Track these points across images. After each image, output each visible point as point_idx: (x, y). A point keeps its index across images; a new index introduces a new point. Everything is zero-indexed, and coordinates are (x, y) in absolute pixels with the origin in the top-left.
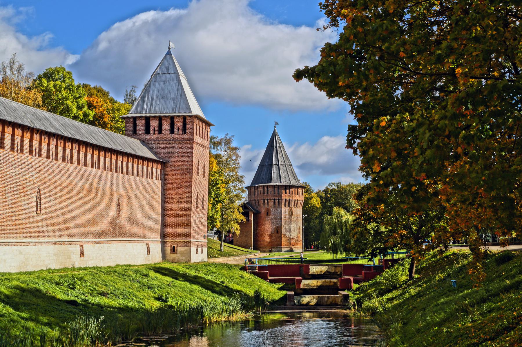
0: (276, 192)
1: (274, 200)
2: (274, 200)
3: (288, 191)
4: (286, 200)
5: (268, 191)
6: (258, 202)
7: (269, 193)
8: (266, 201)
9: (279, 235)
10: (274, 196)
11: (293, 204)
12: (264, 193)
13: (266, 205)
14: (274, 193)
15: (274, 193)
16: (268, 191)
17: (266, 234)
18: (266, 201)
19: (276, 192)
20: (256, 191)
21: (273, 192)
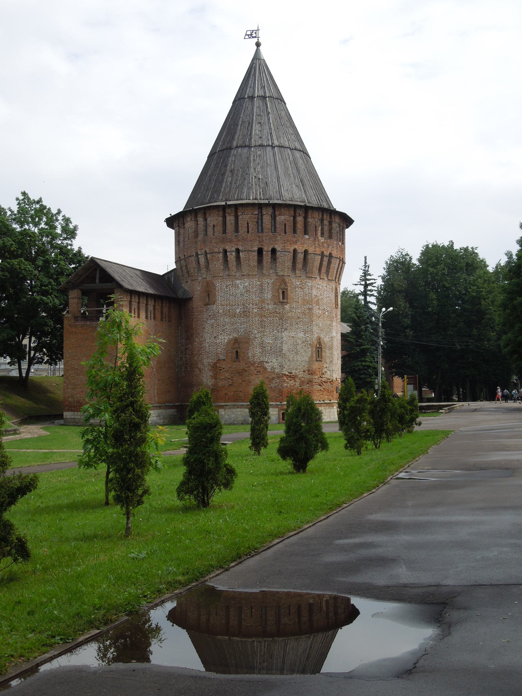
0: (230, 227)
1: (225, 252)
2: (225, 252)
3: (267, 219)
4: (260, 251)
5: (206, 226)
6: (186, 266)
7: (210, 230)
8: (202, 260)
9: (242, 365)
10: (224, 241)
11: (289, 264)
12: (196, 235)
13: (203, 271)
14: (224, 232)
15: (224, 232)
16: (206, 226)
17: (205, 361)
18: (202, 260)
19: (230, 227)
20: (182, 231)
21: (219, 228)
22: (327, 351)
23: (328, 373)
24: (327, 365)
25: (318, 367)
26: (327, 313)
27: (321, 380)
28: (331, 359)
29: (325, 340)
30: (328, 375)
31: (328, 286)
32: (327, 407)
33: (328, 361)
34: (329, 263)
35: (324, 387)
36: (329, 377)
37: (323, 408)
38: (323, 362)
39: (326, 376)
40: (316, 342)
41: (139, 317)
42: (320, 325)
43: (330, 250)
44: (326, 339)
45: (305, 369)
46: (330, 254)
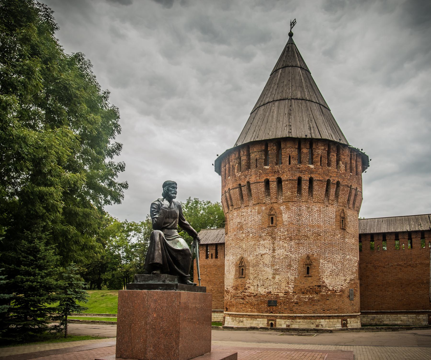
22: (251, 268)
23: (252, 288)
24: (251, 281)
25: (240, 283)
26: (251, 235)
27: (244, 294)
28: (256, 275)
29: (249, 259)
30: (252, 290)
31: (253, 210)
32: (250, 319)
33: (251, 277)
34: (249, 190)
35: (247, 300)
36: (253, 292)
37: (245, 319)
38: (246, 279)
39: (249, 291)
40: (239, 262)
41: (216, 257)
42: (244, 246)
43: (247, 180)
44: (250, 258)
45: (233, 285)
46: (248, 182)
